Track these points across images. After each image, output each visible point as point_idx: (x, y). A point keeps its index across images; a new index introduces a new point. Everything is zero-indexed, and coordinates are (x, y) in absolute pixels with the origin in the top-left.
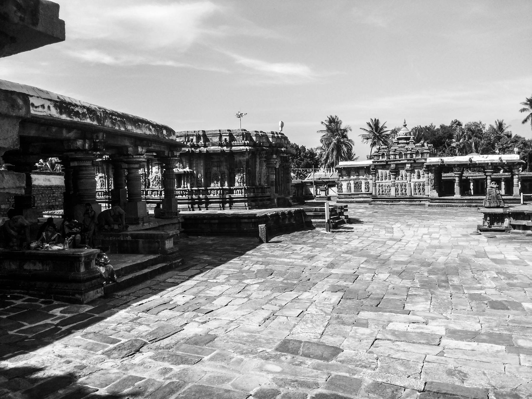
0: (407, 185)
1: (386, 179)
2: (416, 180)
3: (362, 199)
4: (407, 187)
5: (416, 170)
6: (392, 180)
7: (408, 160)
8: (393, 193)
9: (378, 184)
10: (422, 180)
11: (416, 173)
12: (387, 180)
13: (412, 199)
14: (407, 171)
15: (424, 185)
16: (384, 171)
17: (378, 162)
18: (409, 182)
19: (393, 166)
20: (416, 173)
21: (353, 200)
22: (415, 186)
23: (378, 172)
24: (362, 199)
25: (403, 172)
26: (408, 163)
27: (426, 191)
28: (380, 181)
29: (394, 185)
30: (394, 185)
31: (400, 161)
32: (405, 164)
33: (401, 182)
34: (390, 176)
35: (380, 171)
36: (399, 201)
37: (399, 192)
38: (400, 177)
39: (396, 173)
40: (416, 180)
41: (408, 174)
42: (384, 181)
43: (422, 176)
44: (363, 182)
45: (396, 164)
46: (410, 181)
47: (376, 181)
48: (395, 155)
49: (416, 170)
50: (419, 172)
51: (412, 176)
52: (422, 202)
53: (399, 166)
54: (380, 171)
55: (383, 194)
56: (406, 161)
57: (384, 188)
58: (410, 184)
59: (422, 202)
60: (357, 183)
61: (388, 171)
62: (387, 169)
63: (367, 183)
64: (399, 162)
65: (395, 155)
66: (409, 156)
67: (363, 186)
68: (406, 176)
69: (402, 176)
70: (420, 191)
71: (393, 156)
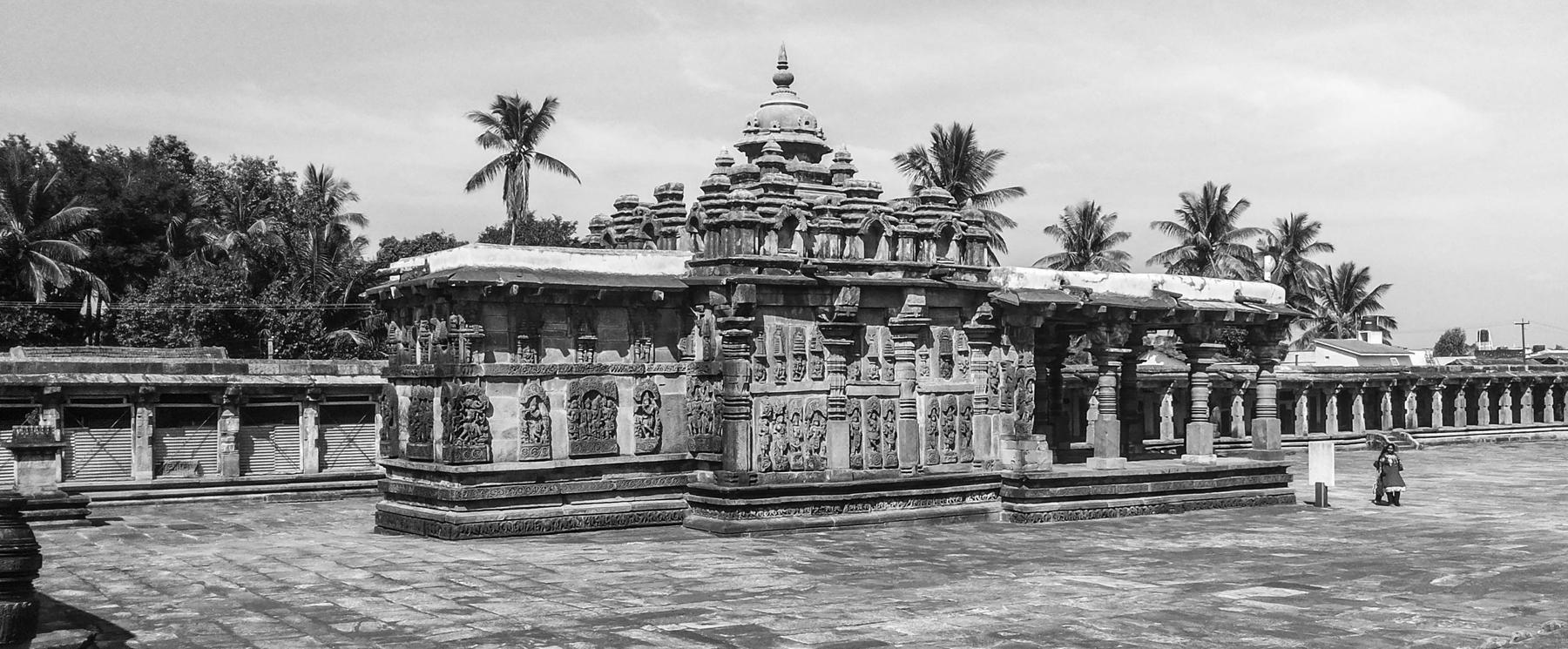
0: (899, 410)
1: (799, 374)
2: (932, 381)
3: (622, 504)
4: (899, 424)
5: (936, 330)
6: (830, 380)
7: (908, 270)
8: (838, 458)
9: (760, 406)
10: (955, 382)
11: (937, 343)
12: (807, 383)
13: (929, 487)
14: (894, 330)
15: (968, 412)
16: (790, 324)
17: (761, 265)
18: (905, 396)
19: (845, 300)
20: (937, 343)
21: (566, 509)
22: (933, 414)
23: (759, 329)
24: (622, 504)
25: (877, 337)
26: (916, 288)
27: (977, 443)
28: (770, 384)
29: (841, 410)
30: (841, 410)
31: (870, 269)
32: (896, 293)
33: (875, 391)
34: (821, 354)
35: (771, 322)
36: (874, 502)
37: (866, 452)
38: (864, 364)
39: (847, 338)
40: (932, 381)
41: (903, 348)
42: (791, 384)
43: (959, 360)
44: (627, 390)
45: (866, 288)
46: (914, 386)
47: (756, 387)
48: (843, 234)
49: (936, 330)
50: (946, 340)
51: (919, 363)
52: (972, 503)
53: (873, 302)
54: (771, 322)
55: (787, 469)
56: (897, 276)
57: (793, 430)
58: (912, 404)
59: (972, 503)
60: (592, 394)
61: (810, 328)
62: (811, 313)
63: (648, 403)
64: (863, 277)
65: (843, 234)
66: (906, 249)
67: (626, 415)
68: (893, 360)
69: (874, 360)
70: (952, 446)
71: (834, 242)
